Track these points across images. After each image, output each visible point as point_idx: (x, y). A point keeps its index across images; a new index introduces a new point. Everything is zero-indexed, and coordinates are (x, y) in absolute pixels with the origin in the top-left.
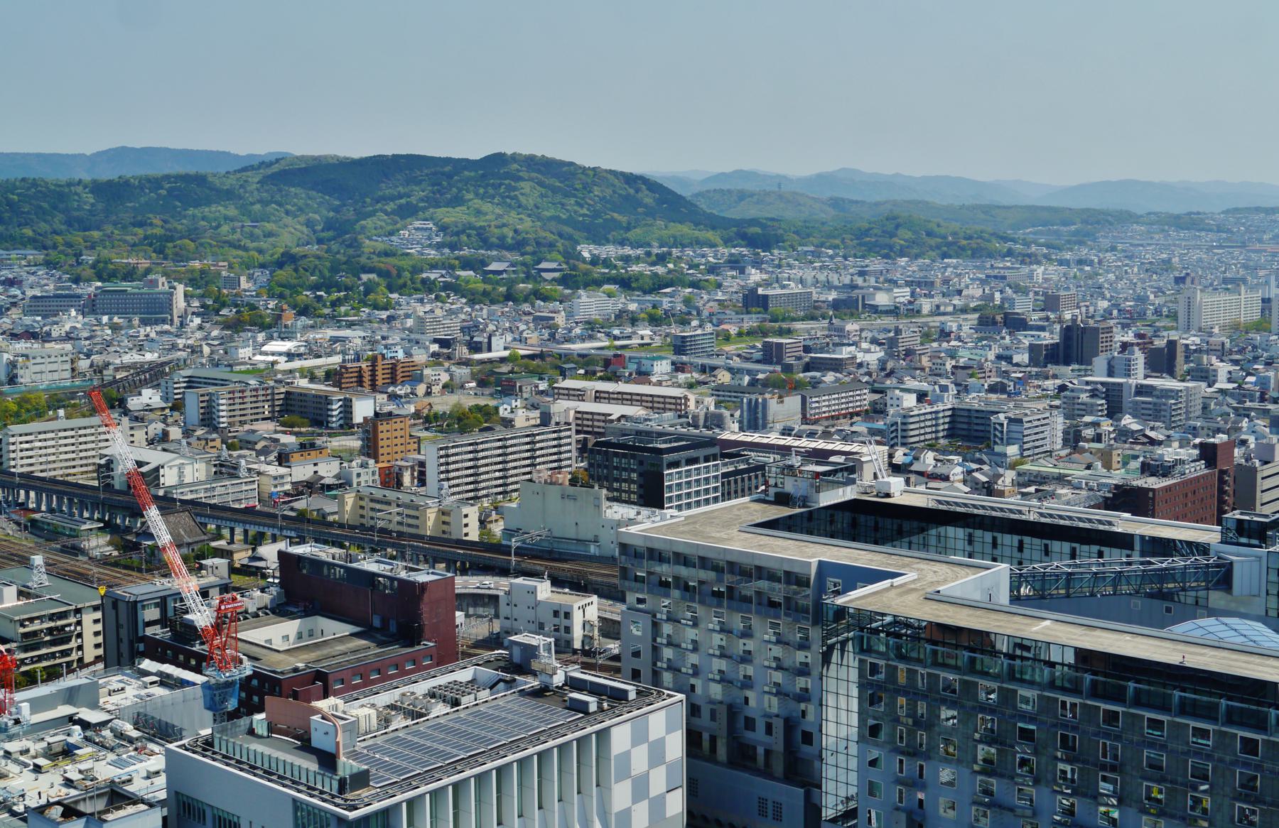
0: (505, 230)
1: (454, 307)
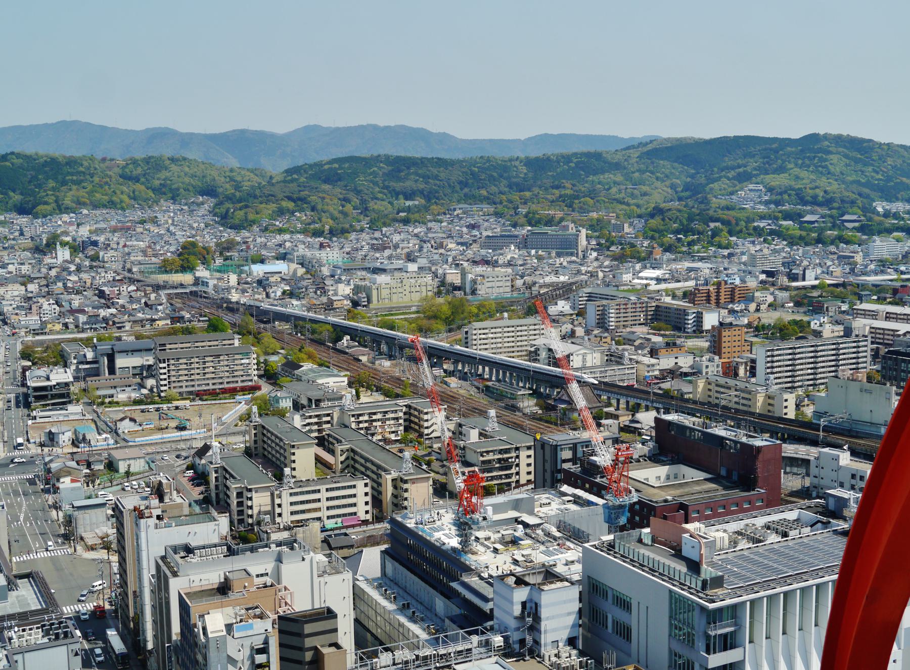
0: (817, 191)
1: (777, 247)
